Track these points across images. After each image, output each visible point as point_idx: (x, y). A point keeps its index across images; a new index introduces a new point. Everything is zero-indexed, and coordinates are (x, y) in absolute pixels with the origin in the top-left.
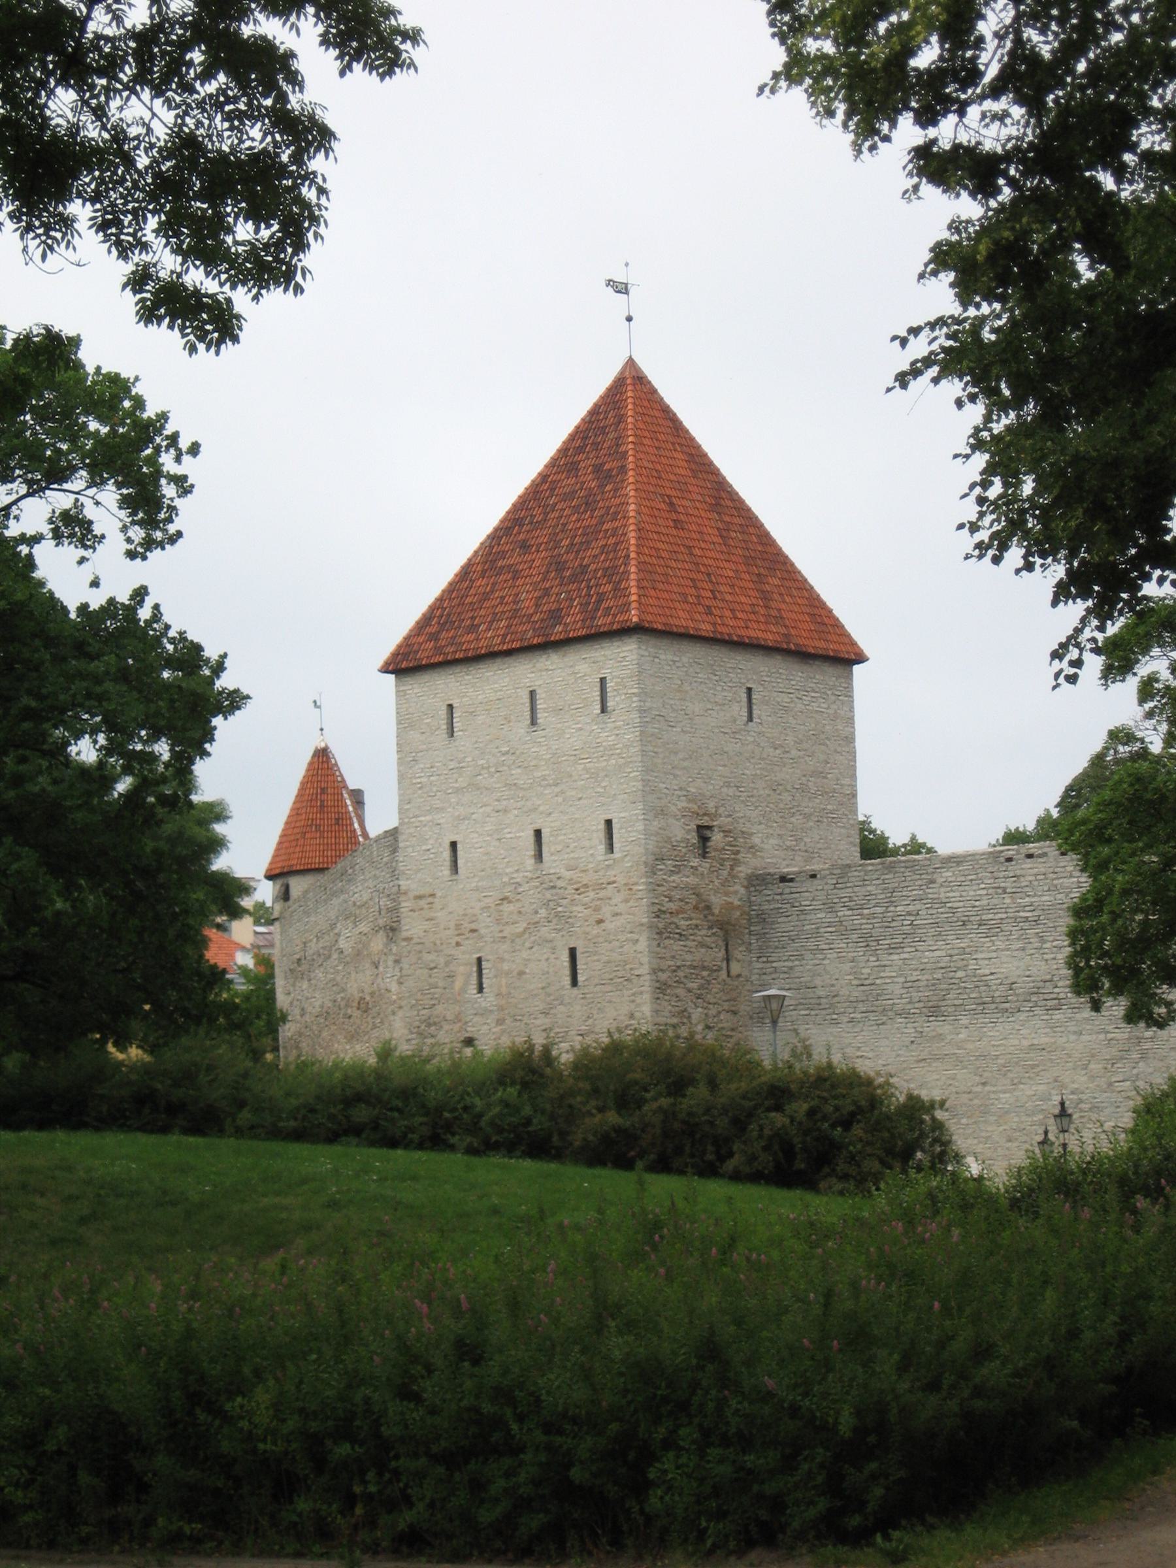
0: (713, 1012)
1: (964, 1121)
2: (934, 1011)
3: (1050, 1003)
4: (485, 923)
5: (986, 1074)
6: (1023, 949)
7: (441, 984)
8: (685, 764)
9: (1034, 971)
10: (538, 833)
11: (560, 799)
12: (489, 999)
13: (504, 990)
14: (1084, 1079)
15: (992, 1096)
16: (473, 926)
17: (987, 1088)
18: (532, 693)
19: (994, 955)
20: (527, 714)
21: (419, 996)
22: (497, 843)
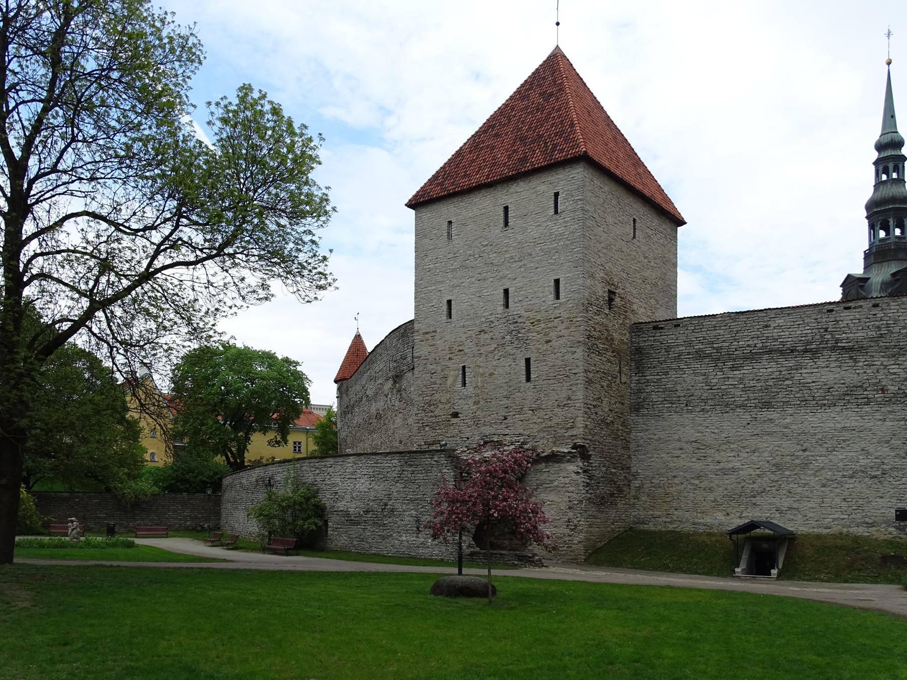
0: (613, 402)
1: (787, 473)
2: (767, 405)
3: (860, 401)
4: (469, 347)
5: (805, 445)
6: (840, 367)
7: (438, 382)
8: (605, 251)
9: (848, 381)
10: (506, 292)
11: (523, 269)
12: (470, 389)
13: (480, 384)
14: (888, 449)
15: (811, 458)
16: (460, 348)
17: (807, 453)
18: (506, 209)
19: (816, 370)
20: (502, 221)
21: (424, 389)
22: (478, 299)
